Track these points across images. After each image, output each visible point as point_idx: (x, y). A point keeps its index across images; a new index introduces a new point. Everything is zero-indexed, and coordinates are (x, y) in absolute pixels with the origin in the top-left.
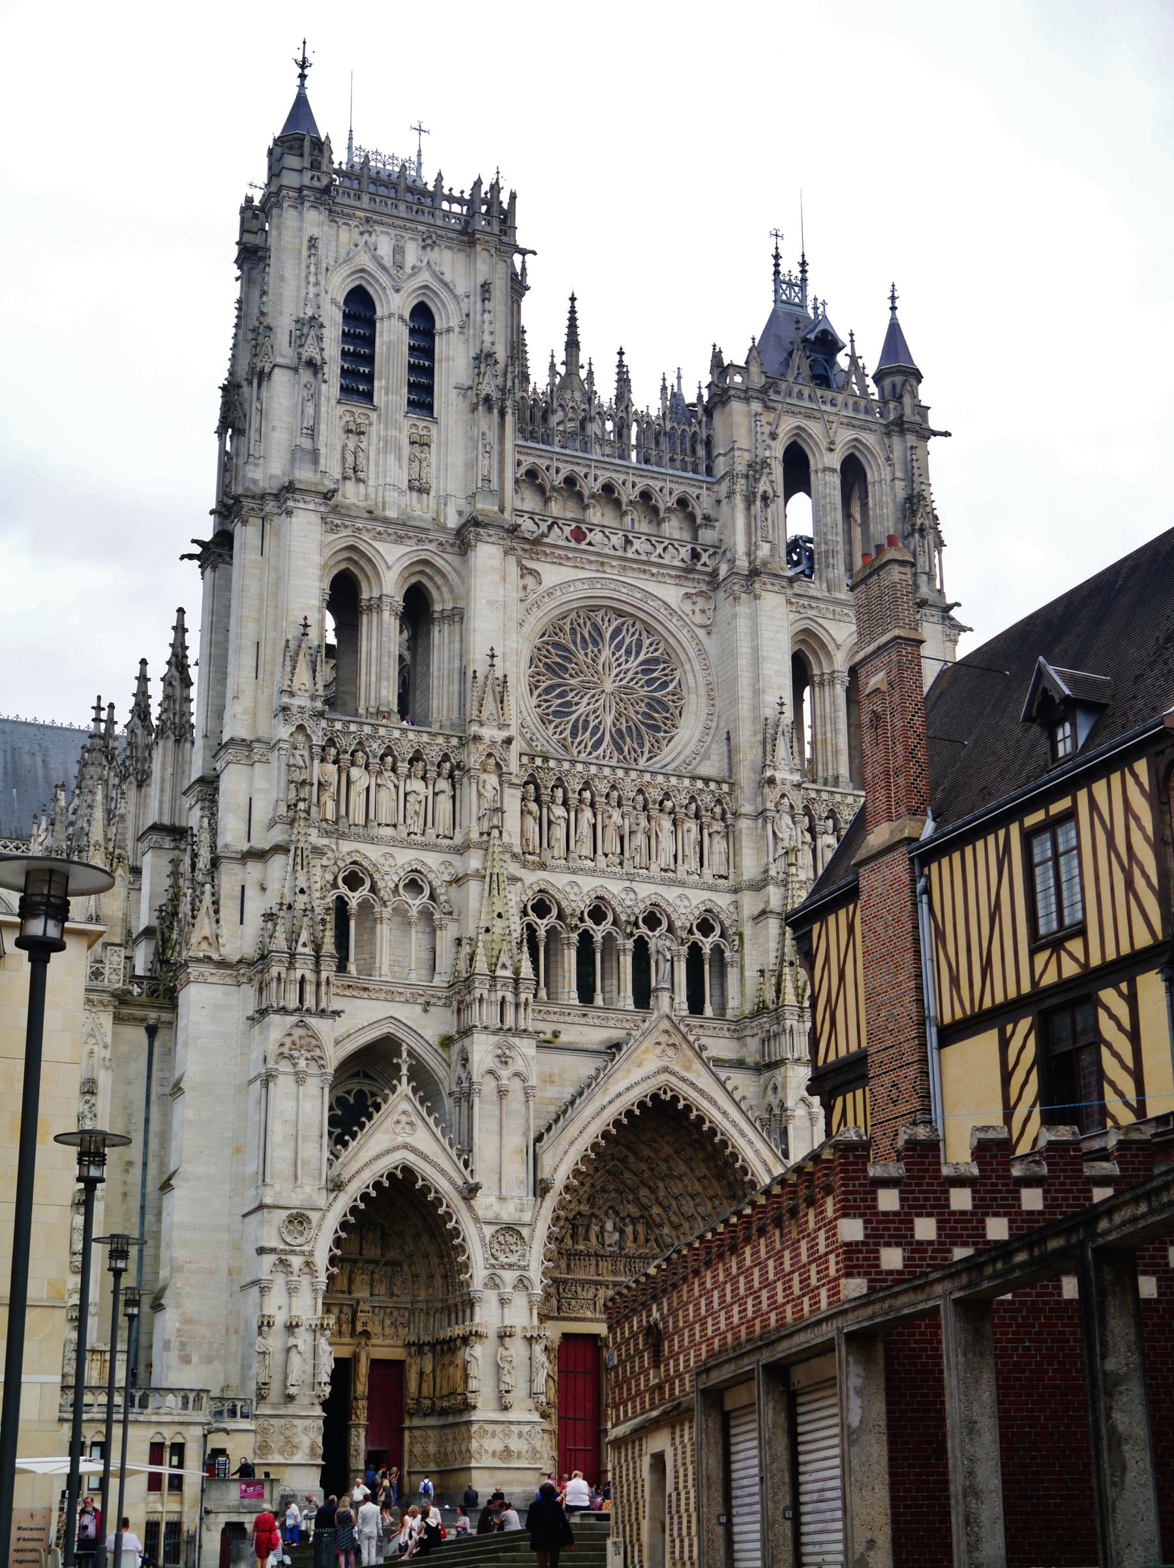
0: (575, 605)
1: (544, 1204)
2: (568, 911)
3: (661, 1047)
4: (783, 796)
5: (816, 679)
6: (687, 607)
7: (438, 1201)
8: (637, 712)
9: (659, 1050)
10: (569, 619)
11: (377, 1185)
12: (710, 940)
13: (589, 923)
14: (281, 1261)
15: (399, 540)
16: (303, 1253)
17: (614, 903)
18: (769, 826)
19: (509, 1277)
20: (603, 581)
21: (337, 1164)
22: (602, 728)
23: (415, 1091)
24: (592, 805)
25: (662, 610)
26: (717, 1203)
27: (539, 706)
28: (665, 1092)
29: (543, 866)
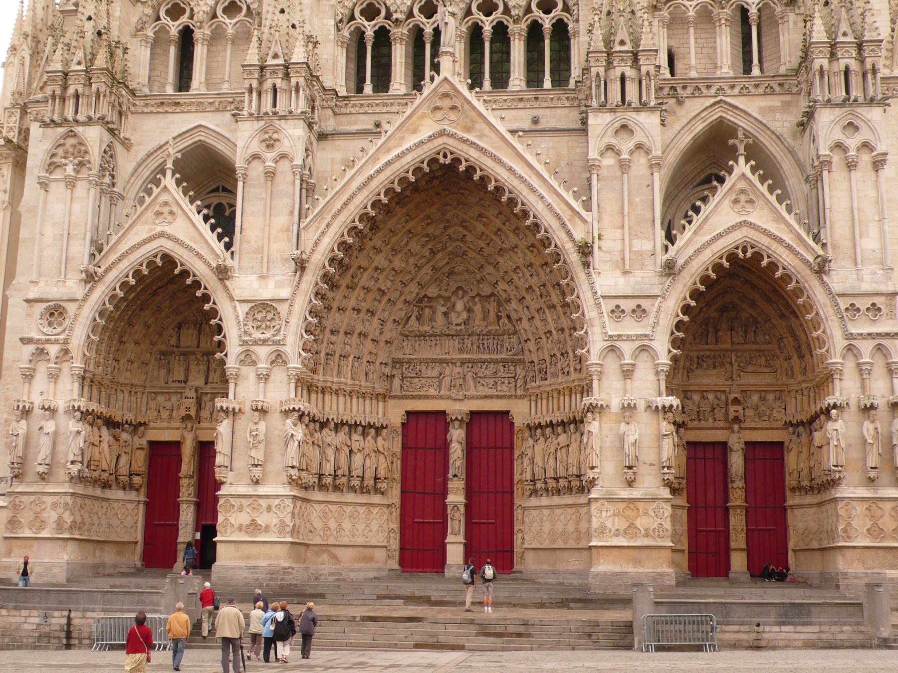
1: (305, 278)
2: (392, 9)
3: (442, 112)
7: (197, 284)
9: (439, 115)
11: (137, 273)
12: (552, 15)
13: (419, 18)
14: (42, 350)
16: (56, 342)
19: (263, 352)
21: (98, 257)
23: (178, 183)
26: (548, 270)
28: (445, 156)
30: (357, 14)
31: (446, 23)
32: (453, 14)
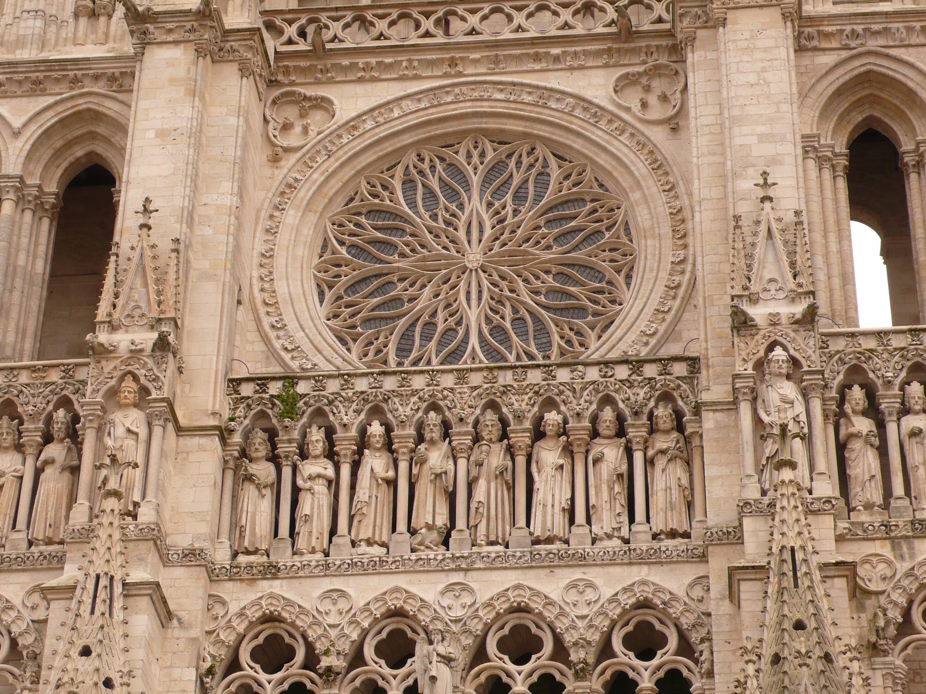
0: (407, 139)
2: (320, 647)
4: (771, 348)
5: (907, 159)
6: (632, 99)
8: (537, 293)
10: (399, 171)
12: (655, 662)
15: (37, 87)
17: (424, 617)
18: (745, 409)
20: (457, 90)
22: (461, 331)
24: (388, 445)
25: (576, 112)
27: (336, 316)
29: (272, 571)
30: (245, 657)
31: (433, 679)
32: (447, 660)
